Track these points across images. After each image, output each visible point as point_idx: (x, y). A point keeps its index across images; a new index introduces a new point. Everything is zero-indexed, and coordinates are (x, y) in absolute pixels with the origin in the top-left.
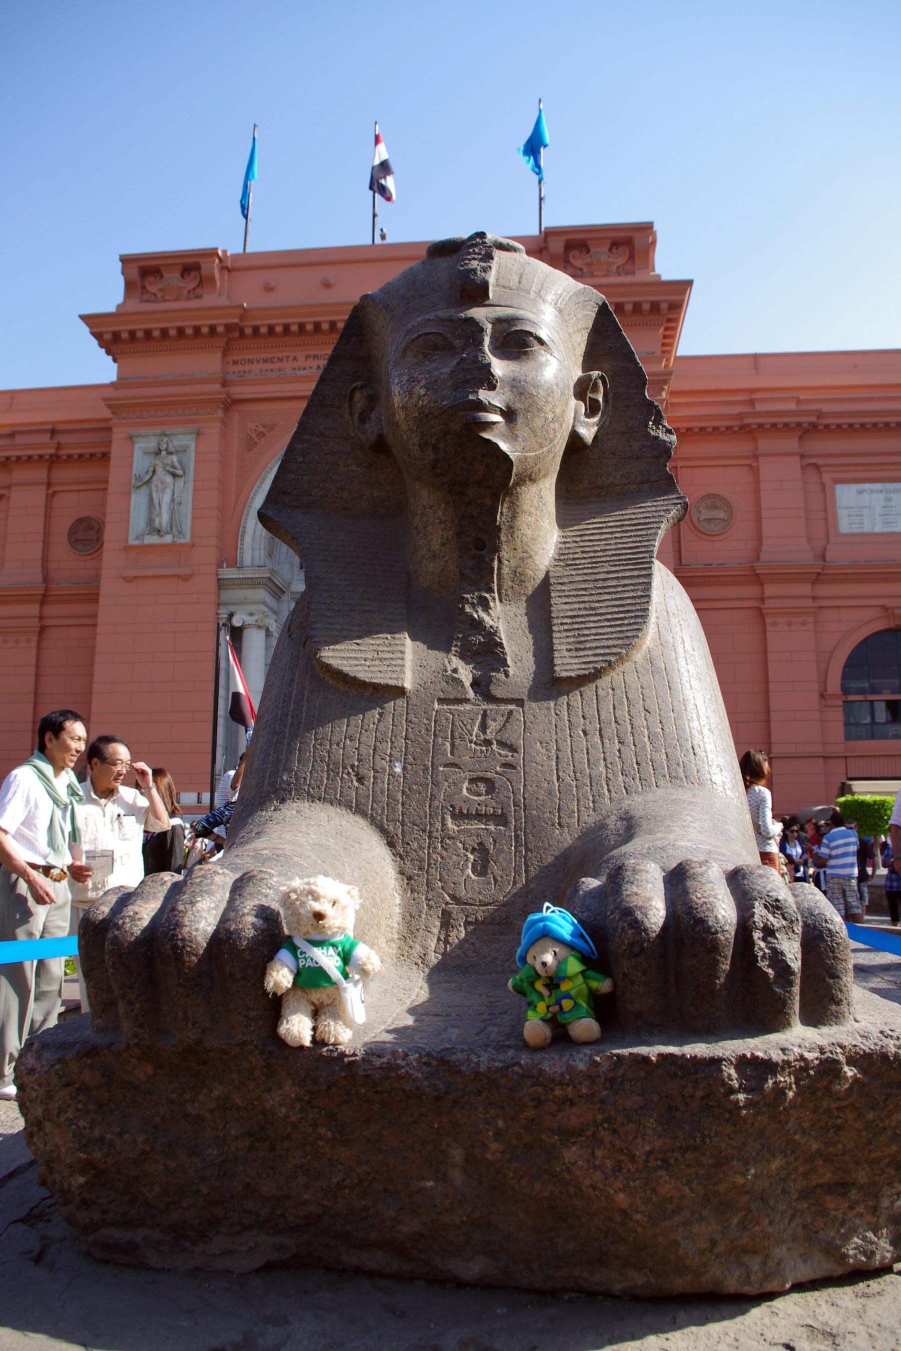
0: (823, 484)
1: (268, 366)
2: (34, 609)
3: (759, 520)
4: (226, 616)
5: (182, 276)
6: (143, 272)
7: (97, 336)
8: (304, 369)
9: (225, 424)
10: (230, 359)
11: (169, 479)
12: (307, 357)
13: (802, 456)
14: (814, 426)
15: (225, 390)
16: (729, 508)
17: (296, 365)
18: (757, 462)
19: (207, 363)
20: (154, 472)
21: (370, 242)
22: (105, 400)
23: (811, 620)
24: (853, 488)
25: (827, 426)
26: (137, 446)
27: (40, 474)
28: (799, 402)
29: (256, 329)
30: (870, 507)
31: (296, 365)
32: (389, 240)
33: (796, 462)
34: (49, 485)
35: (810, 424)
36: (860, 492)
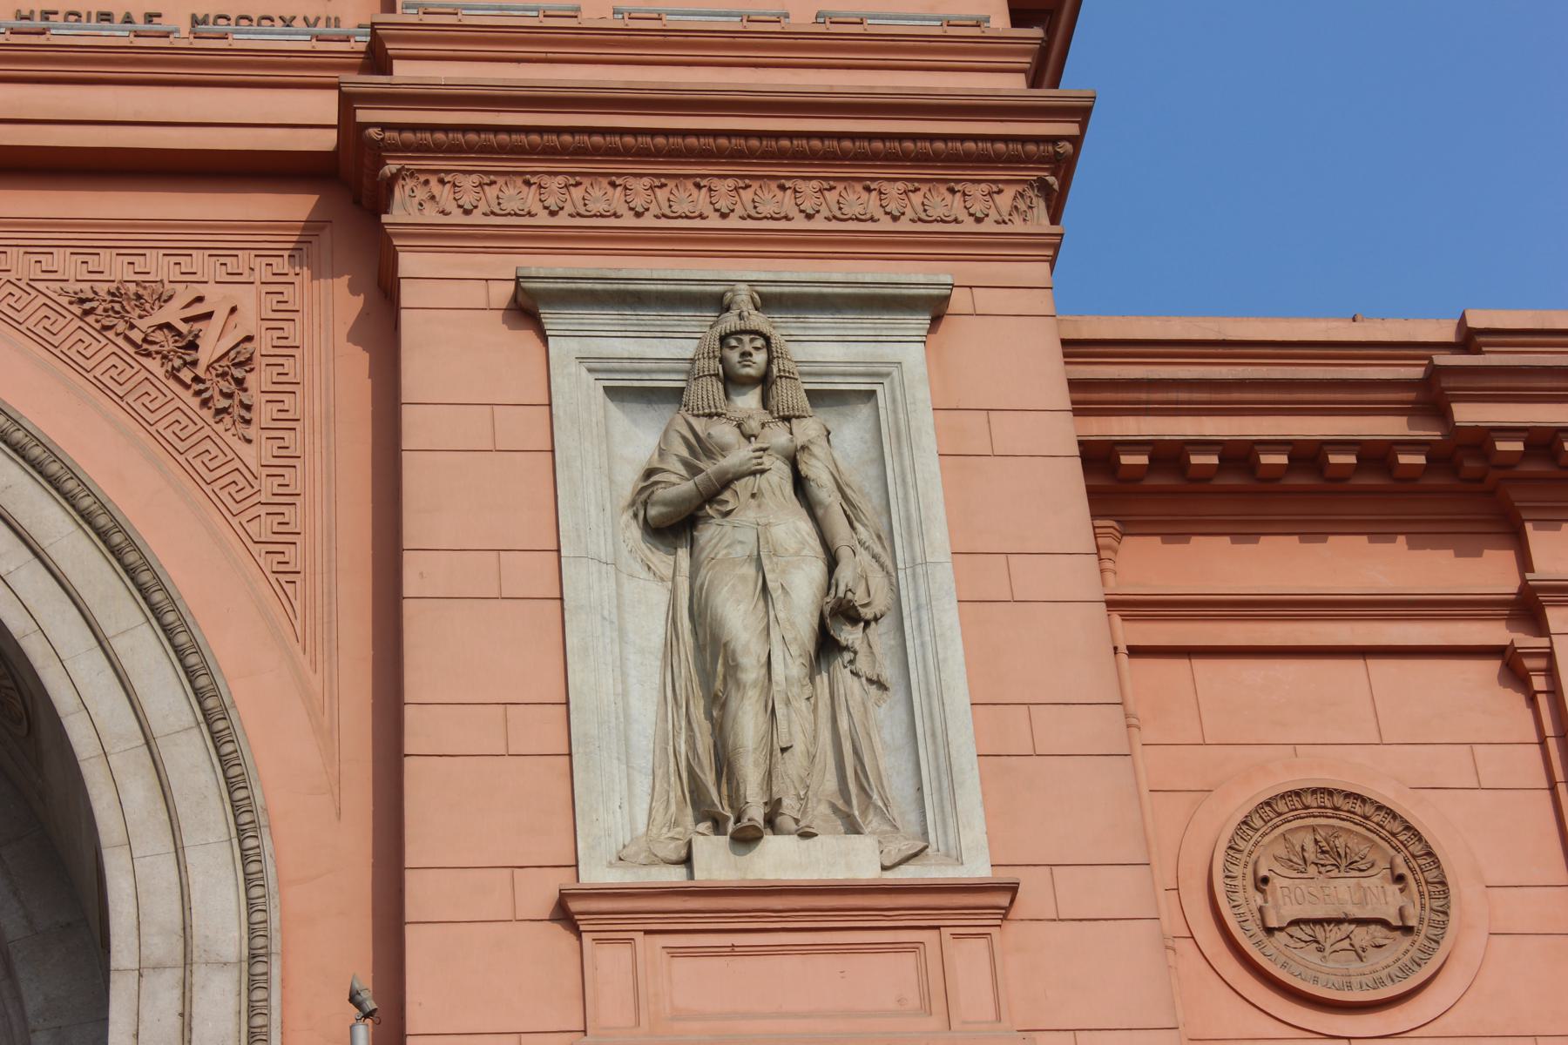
16: (1419, 863)
18: (1541, 628)
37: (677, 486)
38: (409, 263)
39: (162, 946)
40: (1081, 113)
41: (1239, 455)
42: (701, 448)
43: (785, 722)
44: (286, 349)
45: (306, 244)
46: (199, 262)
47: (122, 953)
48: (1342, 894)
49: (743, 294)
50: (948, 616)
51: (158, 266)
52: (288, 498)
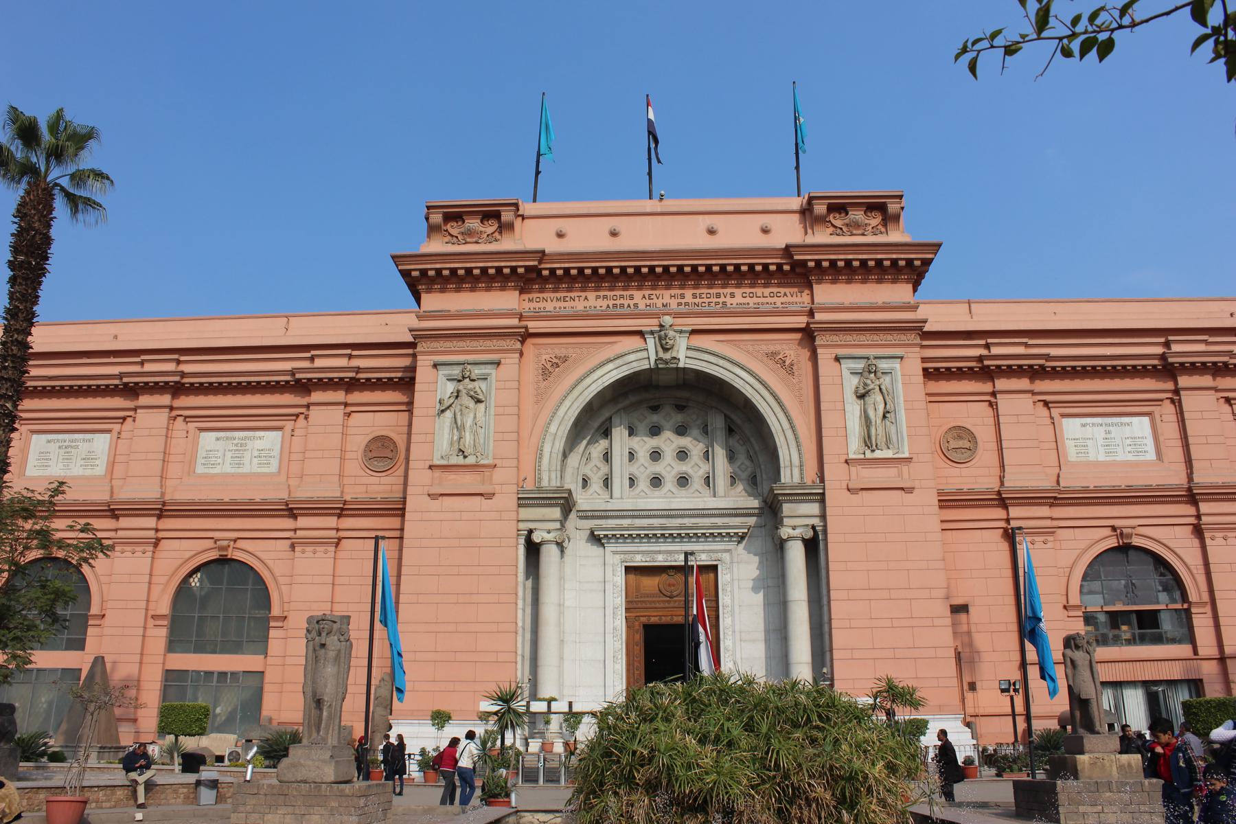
0: (1052, 418)
1: (563, 304)
2: (332, 522)
3: (1000, 450)
7: (405, 274)
9: (521, 354)
10: (526, 296)
11: (471, 404)
12: (598, 297)
13: (1033, 393)
16: (972, 438)
17: (587, 304)
19: (506, 300)
25: (1054, 368)
26: (441, 373)
27: (340, 396)
28: (1026, 345)
29: (553, 271)
31: (587, 304)
33: (1027, 400)
35: (1040, 366)
36: (1084, 425)
37: (862, 391)
38: (819, 351)
39: (788, 463)
40: (925, 322)
41: (948, 369)
42: (865, 384)
43: (878, 430)
44: (799, 362)
45: (800, 342)
46: (784, 346)
47: (782, 464)
48: (961, 443)
50: (903, 413)
51: (778, 348)
52: (801, 389)
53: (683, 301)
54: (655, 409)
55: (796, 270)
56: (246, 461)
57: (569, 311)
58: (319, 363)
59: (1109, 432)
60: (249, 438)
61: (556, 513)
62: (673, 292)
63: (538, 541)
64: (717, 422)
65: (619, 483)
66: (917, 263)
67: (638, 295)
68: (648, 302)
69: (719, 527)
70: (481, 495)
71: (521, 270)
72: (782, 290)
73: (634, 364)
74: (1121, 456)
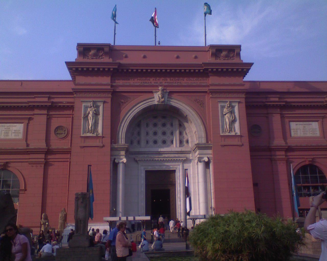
2: (43, 156)
4: (113, 159)
5: (97, 51)
6: (84, 49)
8: (137, 83)
11: (95, 116)
14: (284, 105)
15: (112, 88)
19: (106, 80)
20: (89, 113)
21: (154, 45)
22: (72, 89)
23: (285, 162)
24: (294, 123)
26: (83, 104)
27: (45, 112)
29: (123, 70)
30: (299, 129)
32: (161, 45)
34: (48, 115)
35: (283, 105)
36: (297, 125)
49: (229, 102)
53: (167, 81)
54: (155, 117)
55: (203, 72)
56: (10, 134)
57: (128, 84)
58: (37, 100)
59: (305, 127)
60: (11, 126)
61: (123, 153)
62: (163, 78)
63: (117, 162)
64: (176, 123)
65: (143, 143)
66: (245, 70)
67: (151, 79)
68: (155, 81)
69: (176, 157)
70: (98, 147)
71: (112, 69)
72: (200, 78)
73: (150, 103)
74: (309, 135)
